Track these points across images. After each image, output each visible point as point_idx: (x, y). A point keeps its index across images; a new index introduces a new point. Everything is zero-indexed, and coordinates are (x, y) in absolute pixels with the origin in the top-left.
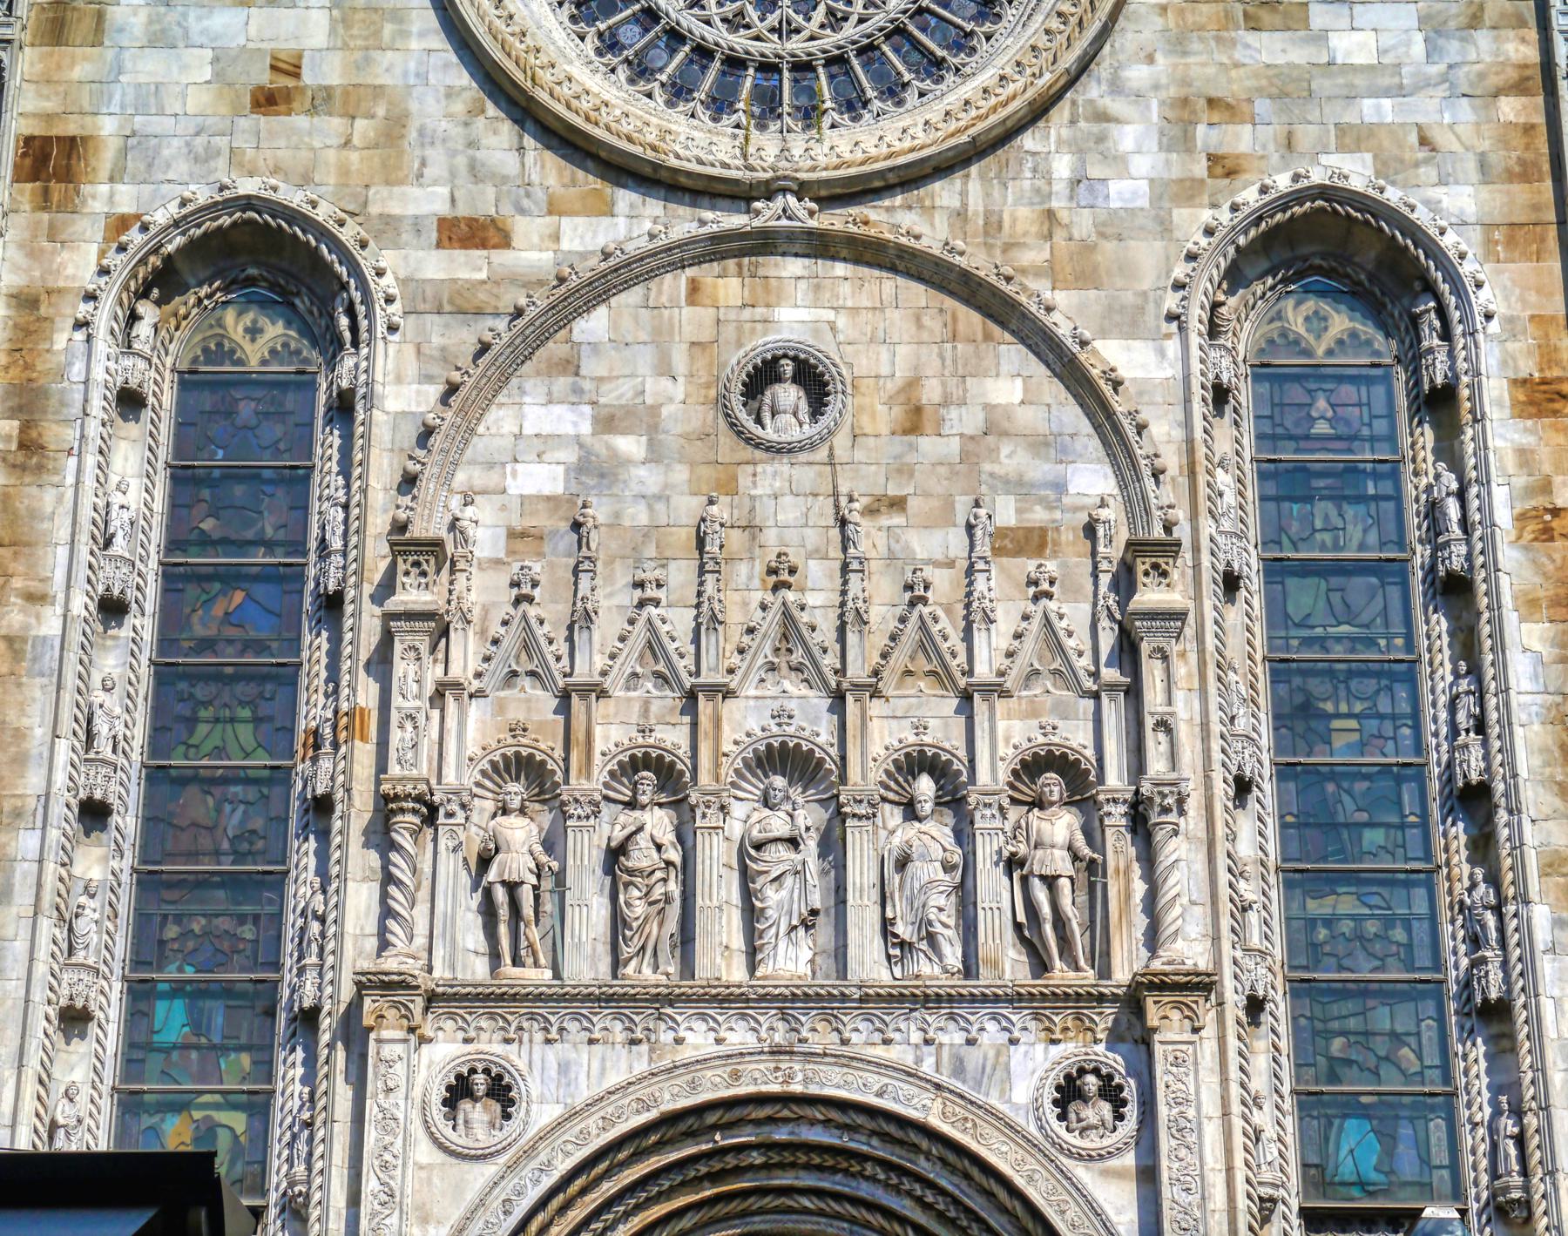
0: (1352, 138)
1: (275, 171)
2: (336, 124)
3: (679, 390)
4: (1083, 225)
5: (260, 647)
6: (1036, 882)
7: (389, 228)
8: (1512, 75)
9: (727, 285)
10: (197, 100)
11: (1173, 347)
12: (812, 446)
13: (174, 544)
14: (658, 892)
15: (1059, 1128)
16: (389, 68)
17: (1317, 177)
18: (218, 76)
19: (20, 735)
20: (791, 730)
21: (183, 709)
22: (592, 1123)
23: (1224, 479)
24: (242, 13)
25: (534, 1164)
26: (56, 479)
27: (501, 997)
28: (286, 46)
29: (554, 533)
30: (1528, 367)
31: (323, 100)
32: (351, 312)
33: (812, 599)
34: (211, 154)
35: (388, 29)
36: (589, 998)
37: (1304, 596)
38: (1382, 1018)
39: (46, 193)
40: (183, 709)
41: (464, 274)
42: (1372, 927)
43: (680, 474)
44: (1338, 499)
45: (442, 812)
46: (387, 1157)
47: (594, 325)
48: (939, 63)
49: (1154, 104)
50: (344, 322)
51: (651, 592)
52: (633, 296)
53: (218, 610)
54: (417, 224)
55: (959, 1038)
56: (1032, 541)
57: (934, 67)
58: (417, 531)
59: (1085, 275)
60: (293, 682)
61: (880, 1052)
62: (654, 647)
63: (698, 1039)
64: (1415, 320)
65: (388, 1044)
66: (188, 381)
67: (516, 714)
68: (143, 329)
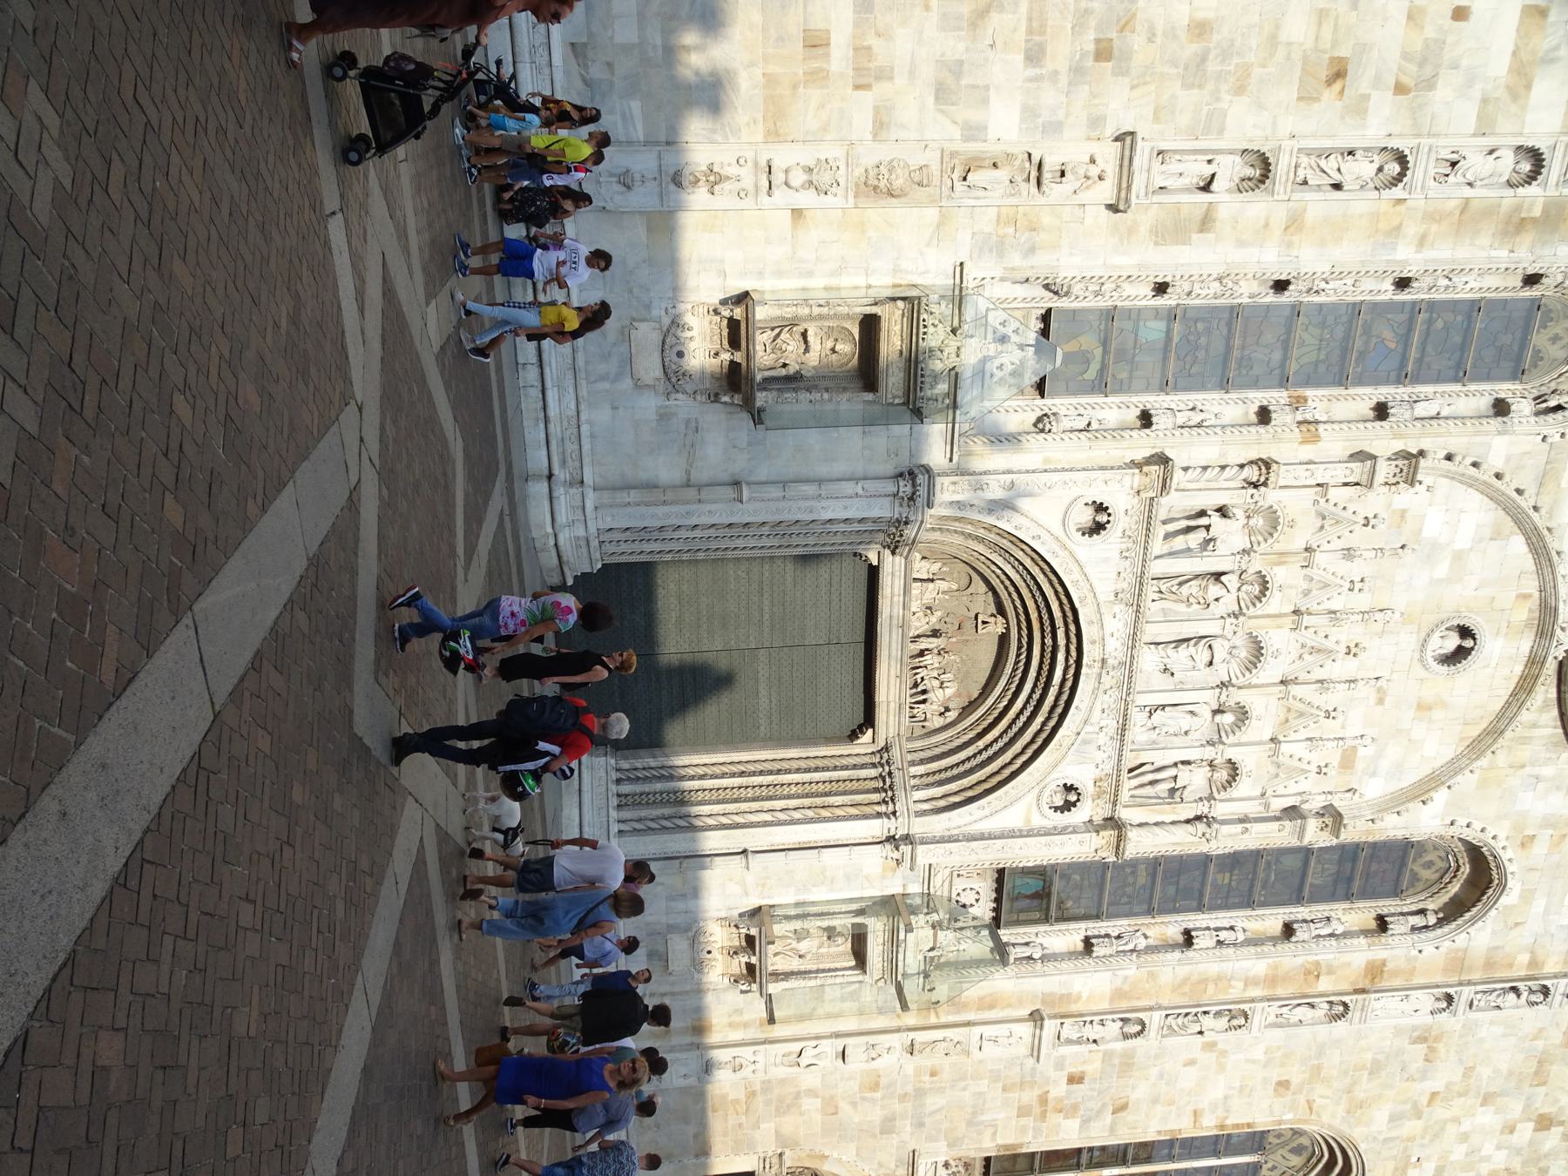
9: (1524, 613)
11: (1438, 822)
12: (1421, 660)
14: (1191, 600)
15: (1053, 786)
17: (1513, 884)
20: (1269, 658)
22: (1077, 575)
25: (1057, 549)
26: (1496, 245)
30: (1390, 966)
36: (1143, 572)
42: (1129, 890)
45: (1255, 491)
46: (1071, 484)
47: (1518, 544)
51: (1358, 586)
52: (1529, 563)
55: (1101, 742)
56: (1348, 761)
61: (1098, 707)
64: (1422, 912)
65: (1134, 479)
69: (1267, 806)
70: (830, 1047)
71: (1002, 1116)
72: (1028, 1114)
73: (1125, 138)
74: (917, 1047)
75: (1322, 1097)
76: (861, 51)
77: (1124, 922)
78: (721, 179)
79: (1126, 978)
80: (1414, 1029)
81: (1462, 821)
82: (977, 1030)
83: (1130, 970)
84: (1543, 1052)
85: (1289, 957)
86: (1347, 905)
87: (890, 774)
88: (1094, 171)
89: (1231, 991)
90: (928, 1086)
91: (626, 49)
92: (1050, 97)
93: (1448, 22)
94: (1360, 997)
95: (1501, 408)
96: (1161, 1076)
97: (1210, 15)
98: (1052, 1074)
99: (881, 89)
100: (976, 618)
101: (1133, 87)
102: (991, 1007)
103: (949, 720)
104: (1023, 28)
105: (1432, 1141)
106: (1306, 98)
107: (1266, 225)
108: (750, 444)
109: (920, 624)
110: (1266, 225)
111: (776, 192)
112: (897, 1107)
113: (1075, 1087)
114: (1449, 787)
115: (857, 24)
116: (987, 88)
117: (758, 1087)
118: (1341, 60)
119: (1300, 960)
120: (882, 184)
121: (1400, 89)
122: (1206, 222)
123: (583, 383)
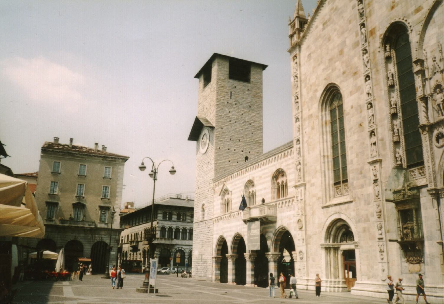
2: (400, 6)
54: (412, 13)
88: (374, 168)
93: (353, 108)
110: (382, 126)
121: (361, 112)
122: (382, 140)
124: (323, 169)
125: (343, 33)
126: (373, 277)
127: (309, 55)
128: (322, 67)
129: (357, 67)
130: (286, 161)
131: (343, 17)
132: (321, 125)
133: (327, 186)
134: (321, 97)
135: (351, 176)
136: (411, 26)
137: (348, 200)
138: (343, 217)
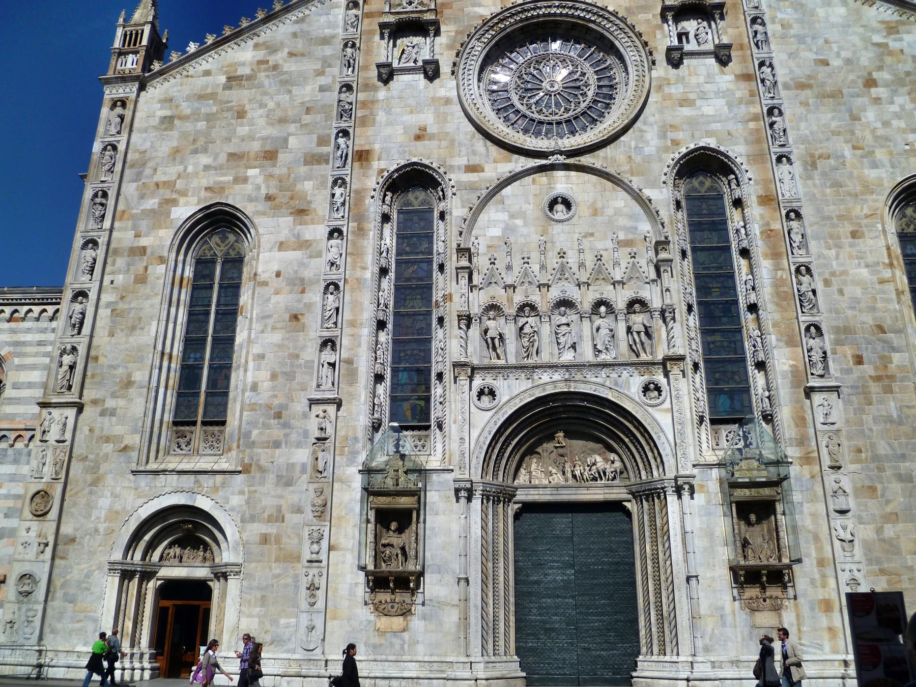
0: (709, 134)
1: (421, 155)
2: (435, 143)
3: (531, 207)
4: (638, 159)
5: (421, 279)
6: (635, 333)
7: (451, 167)
8: (752, 116)
9: (542, 178)
10: (400, 139)
11: (665, 190)
12: (568, 220)
13: (398, 254)
15: (644, 398)
16: (450, 128)
17: (702, 144)
18: (405, 132)
19: (361, 304)
21: (403, 297)
22: (517, 400)
23: (680, 226)
24: (410, 116)
27: (492, 368)
28: (422, 124)
29: (499, 246)
30: (761, 192)
31: (432, 137)
32: (442, 190)
33: (570, 261)
34: (404, 152)
35: (449, 117)
36: (515, 367)
37: (702, 256)
38: (730, 367)
39: (362, 164)
40: (403, 297)
41: (473, 179)
43: (533, 229)
44: (710, 230)
48: (596, 120)
49: (656, 128)
50: (441, 193)
51: (526, 260)
53: (410, 270)
55: (616, 376)
57: (594, 121)
58: (462, 246)
59: (640, 173)
60: (431, 288)
61: (594, 379)
62: (526, 274)
63: (545, 377)
64: (729, 184)
66: (399, 212)
67: (492, 293)
68: (388, 198)
69: (653, 281)
70: (838, 522)
71: (892, 404)
72: (890, 387)
73: (313, 402)
74: (834, 464)
75: (862, 211)
76: (270, 520)
77: (746, 344)
78: (312, 584)
79: (778, 340)
80: (805, 169)
81: (664, 178)
82: (819, 427)
83: (772, 339)
84: (817, 97)
85: (759, 248)
86: (729, 222)
87: (644, 491)
88: (322, 415)
89: (784, 277)
90: (870, 454)
91: (261, 623)
92: (294, 437)
93: (281, 278)
94: (781, 205)
95: (442, 216)
96: (853, 308)
97: (269, 373)
98: (855, 376)
99: (284, 510)
100: (556, 447)
101: (293, 401)
102: (803, 419)
103: (617, 458)
104: (267, 450)
105: (890, 141)
106: (303, 329)
107: (352, 335)
108: (439, 573)
109: (558, 479)
110: (352, 335)
111: (321, 558)
112: (888, 473)
113: (865, 360)
114: (640, 190)
115: (259, 522)
116: (288, 464)
117: (876, 568)
118: (290, 317)
119: (760, 243)
120: (320, 509)
121: (303, 292)
122: (349, 362)
123: (404, 658)
124: (154, 384)
125: (282, 121)
126: (271, 644)
127: (168, 122)
128: (205, 160)
129: (310, 202)
130: (13, 331)
131: (290, 92)
132: (170, 281)
133: (157, 424)
134: (184, 222)
135: (235, 416)
136: (453, 187)
137: (224, 466)
138: (203, 503)
